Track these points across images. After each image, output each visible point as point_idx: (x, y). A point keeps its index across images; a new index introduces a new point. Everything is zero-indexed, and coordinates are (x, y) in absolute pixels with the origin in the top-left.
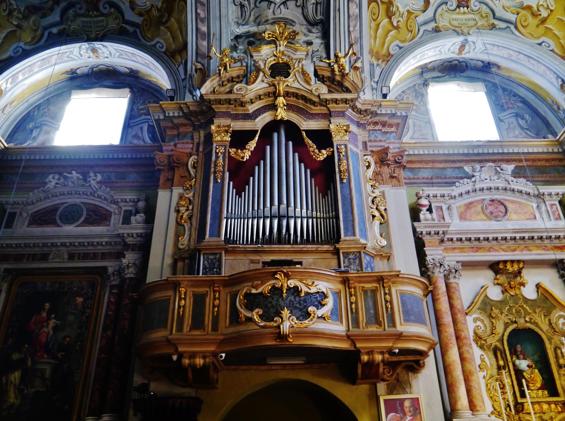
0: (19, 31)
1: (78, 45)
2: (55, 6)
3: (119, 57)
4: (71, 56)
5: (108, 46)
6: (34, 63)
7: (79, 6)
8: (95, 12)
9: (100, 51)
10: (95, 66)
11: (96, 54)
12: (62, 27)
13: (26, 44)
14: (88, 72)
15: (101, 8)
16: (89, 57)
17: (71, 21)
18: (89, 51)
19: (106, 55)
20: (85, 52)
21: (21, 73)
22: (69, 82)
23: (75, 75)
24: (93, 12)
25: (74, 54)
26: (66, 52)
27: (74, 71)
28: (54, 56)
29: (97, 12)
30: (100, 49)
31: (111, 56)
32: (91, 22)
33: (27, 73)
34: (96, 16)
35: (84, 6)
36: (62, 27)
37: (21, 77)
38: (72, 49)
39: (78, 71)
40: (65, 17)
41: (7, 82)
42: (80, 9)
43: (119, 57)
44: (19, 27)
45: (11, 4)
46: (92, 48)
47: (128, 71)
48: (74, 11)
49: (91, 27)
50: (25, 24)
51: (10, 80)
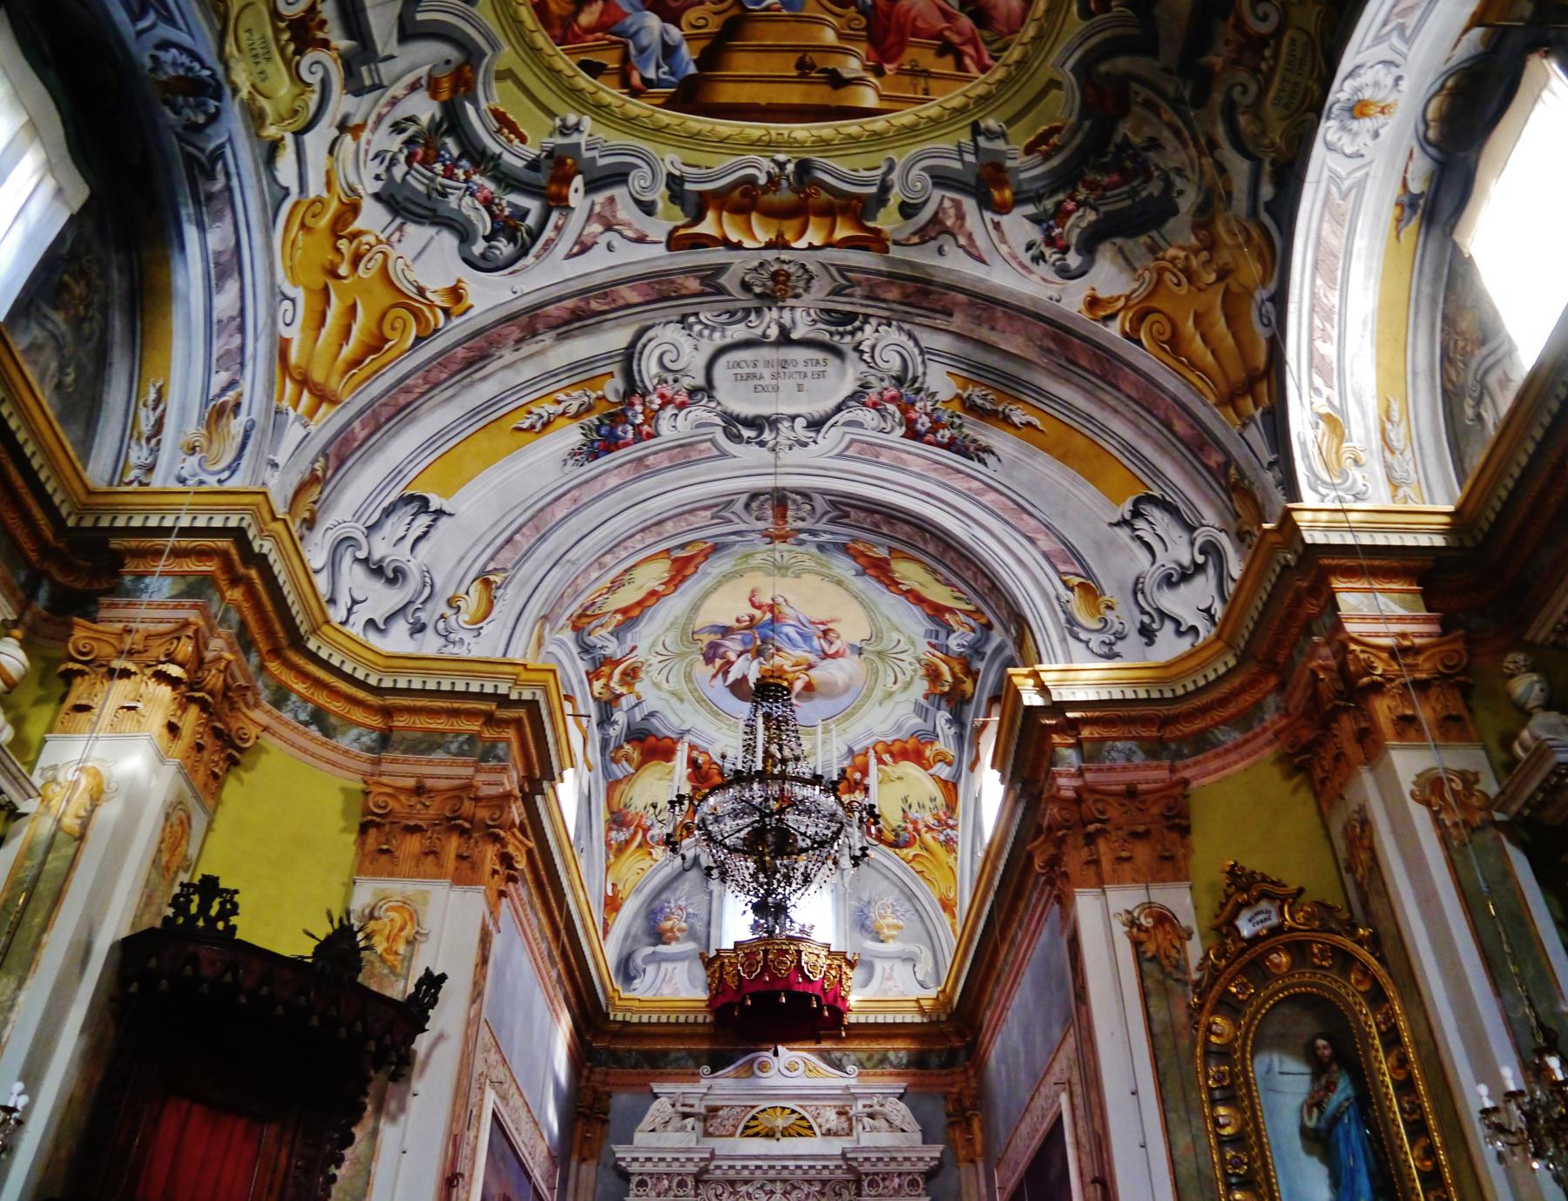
0: (1230, 280)
1: (1318, 150)
2: (1217, 154)
3: (1408, 41)
4: (1346, 185)
5: (1359, 60)
6: (1313, 295)
7: (1238, 89)
8: (1267, 53)
9: (1367, 94)
10: (1421, 128)
11: (1373, 110)
12: (1267, 168)
13: (1264, 283)
14: (1432, 158)
15: (1264, 28)
16: (1376, 135)
17: (1263, 133)
18: (1355, 125)
19: (1389, 81)
20: (1352, 142)
21: (1318, 343)
22: (1436, 232)
23: (1422, 202)
24: (1263, 59)
25: (1344, 174)
26: (1328, 192)
27: (1406, 200)
28: (1324, 233)
29: (1267, 45)
30: (1358, 90)
31: (1397, 66)
32: (1284, 80)
33: (1328, 326)
34: (1276, 56)
35: (1242, 76)
36: (1267, 168)
37: (1328, 350)
38: (1326, 173)
39: (1415, 187)
40: (1251, 148)
41: (1317, 391)
42: (1245, 91)
43: (1408, 41)
44: (1223, 274)
45: (1173, 260)
46: (1347, 114)
47: (1477, 32)
48: (1244, 113)
49: (1296, 84)
50: (1224, 257)
51: (1318, 381)
